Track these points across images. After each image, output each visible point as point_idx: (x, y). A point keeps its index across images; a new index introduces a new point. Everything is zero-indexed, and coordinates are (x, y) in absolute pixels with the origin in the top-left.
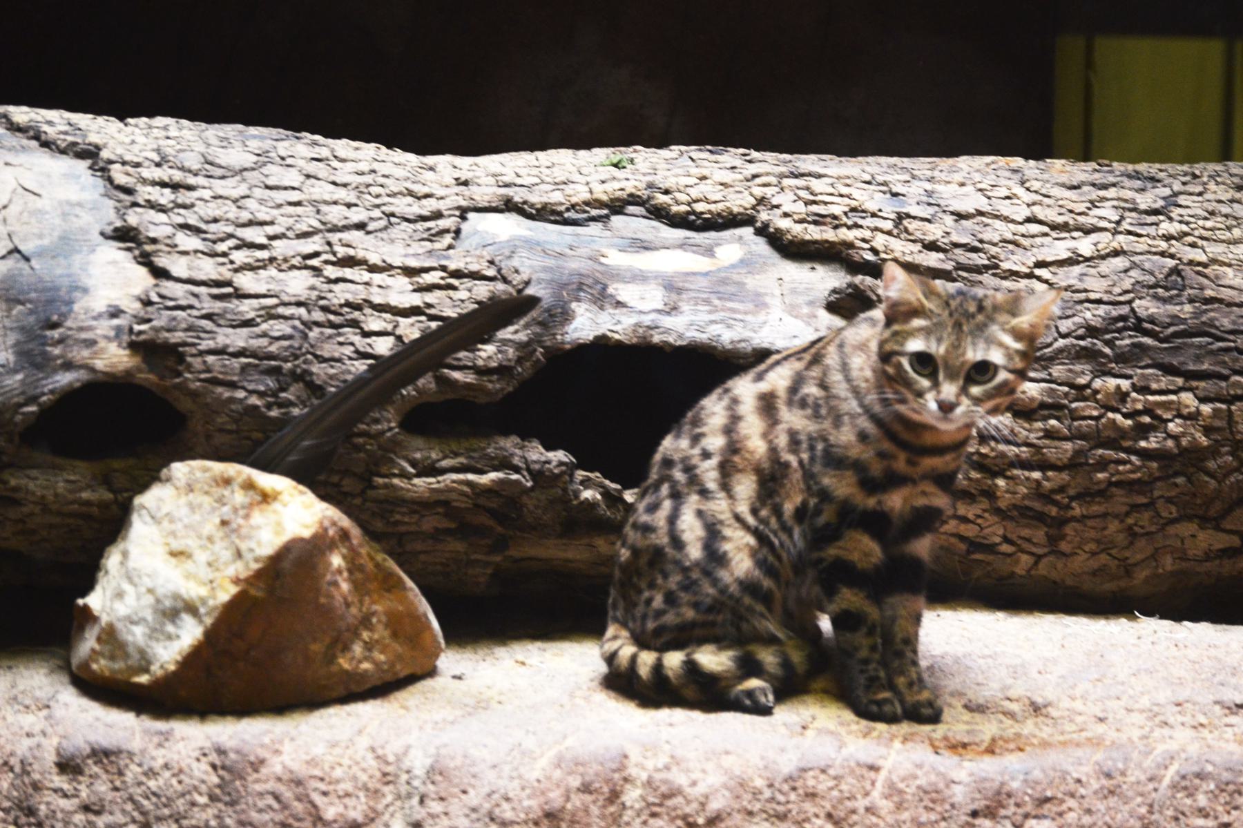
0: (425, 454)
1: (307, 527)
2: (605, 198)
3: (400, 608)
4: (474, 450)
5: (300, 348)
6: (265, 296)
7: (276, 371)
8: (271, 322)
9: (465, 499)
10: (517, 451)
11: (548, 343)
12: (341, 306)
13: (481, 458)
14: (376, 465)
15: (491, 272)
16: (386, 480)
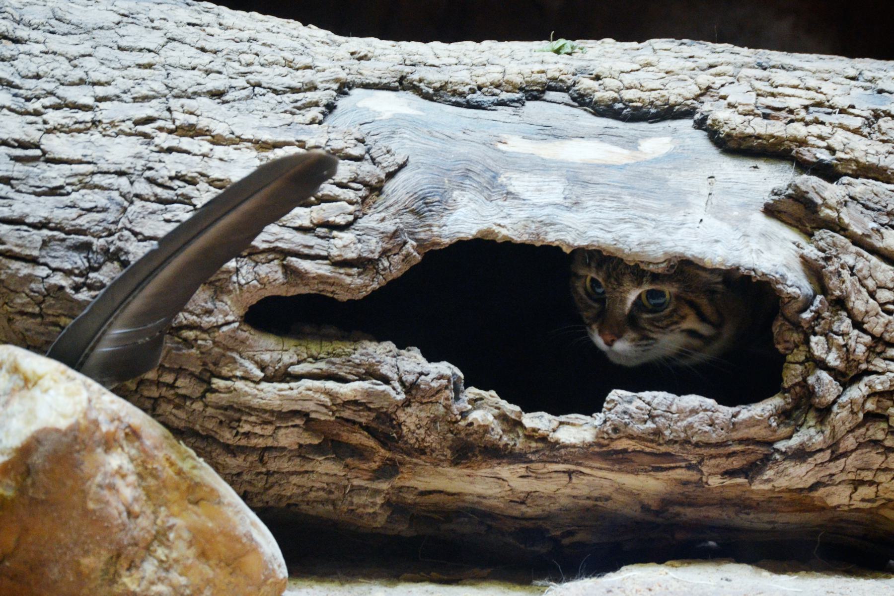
0: (276, 356)
1: (64, 416)
2: (518, 80)
3: (210, 525)
4: (339, 356)
5: (115, 223)
6: (80, 162)
7: (85, 247)
8: (82, 191)
9: (325, 410)
10: (389, 359)
11: (422, 236)
12: (171, 178)
13: (343, 364)
14: (216, 364)
15: (358, 151)
16: (229, 383)
